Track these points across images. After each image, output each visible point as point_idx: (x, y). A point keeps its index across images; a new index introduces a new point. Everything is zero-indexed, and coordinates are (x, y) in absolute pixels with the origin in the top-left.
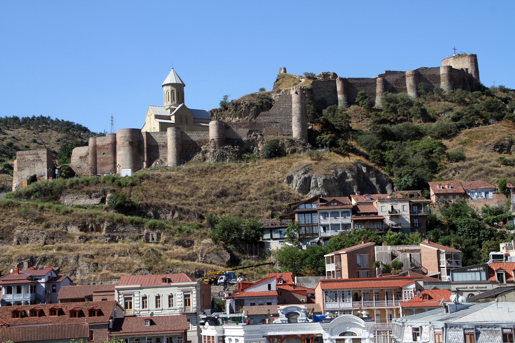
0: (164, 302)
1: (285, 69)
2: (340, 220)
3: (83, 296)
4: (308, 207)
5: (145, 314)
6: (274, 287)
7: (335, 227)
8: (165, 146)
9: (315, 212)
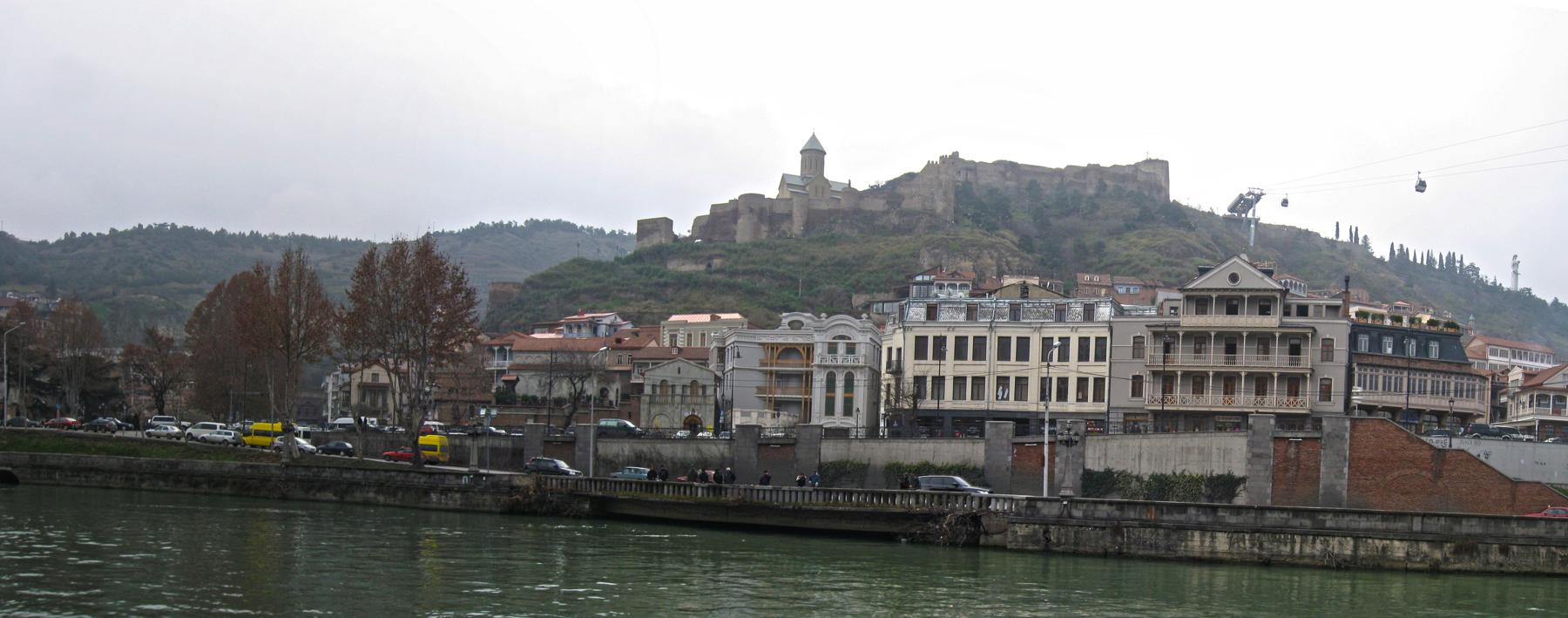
8: (789, 216)
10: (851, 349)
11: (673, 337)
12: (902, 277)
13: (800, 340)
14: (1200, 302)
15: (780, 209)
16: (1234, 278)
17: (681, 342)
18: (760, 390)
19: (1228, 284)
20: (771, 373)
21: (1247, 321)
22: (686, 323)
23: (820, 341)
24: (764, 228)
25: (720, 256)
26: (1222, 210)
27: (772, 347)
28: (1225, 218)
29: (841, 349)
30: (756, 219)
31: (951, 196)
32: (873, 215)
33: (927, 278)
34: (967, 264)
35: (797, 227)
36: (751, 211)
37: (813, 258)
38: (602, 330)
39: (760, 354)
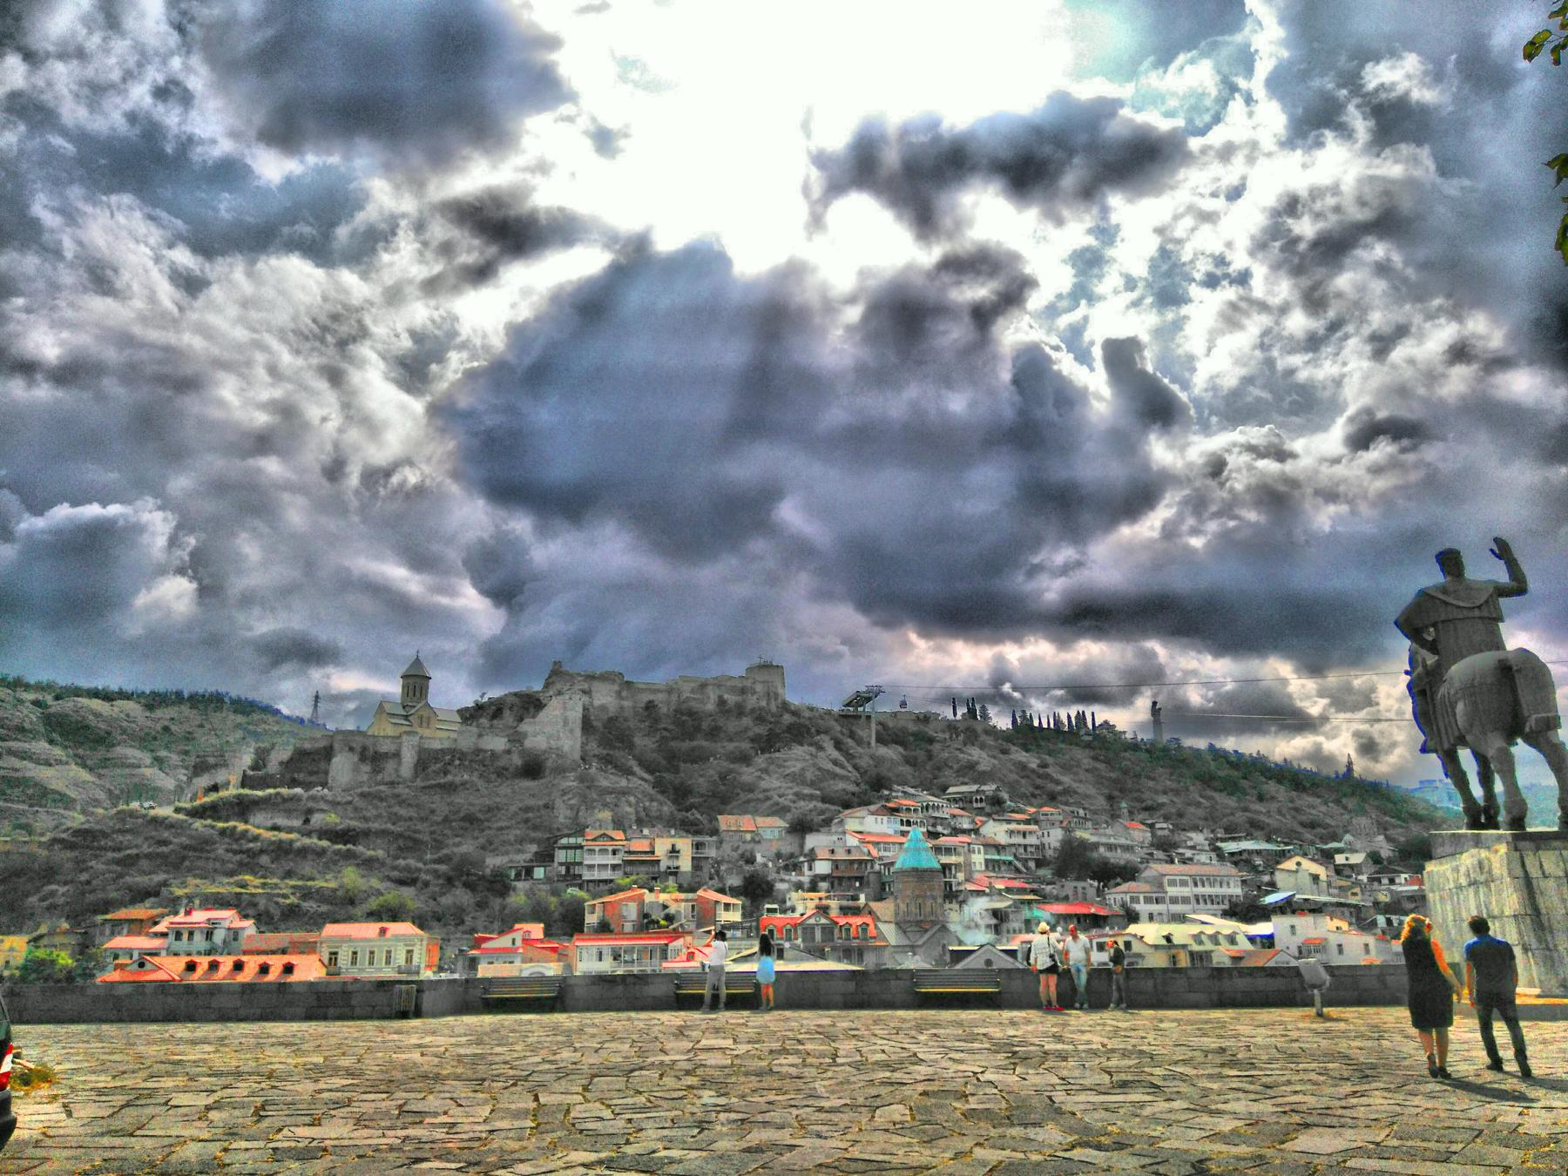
0: (380, 957)
3: (274, 948)
4: (572, 840)
5: (354, 973)
6: (519, 943)
8: (397, 755)
9: (581, 847)
11: (334, 955)
17: (344, 960)
22: (348, 939)
24: (366, 768)
26: (836, 708)
30: (356, 758)
31: (578, 733)
33: (572, 840)
34: (606, 815)
35: (406, 769)
37: (433, 812)
38: (219, 936)
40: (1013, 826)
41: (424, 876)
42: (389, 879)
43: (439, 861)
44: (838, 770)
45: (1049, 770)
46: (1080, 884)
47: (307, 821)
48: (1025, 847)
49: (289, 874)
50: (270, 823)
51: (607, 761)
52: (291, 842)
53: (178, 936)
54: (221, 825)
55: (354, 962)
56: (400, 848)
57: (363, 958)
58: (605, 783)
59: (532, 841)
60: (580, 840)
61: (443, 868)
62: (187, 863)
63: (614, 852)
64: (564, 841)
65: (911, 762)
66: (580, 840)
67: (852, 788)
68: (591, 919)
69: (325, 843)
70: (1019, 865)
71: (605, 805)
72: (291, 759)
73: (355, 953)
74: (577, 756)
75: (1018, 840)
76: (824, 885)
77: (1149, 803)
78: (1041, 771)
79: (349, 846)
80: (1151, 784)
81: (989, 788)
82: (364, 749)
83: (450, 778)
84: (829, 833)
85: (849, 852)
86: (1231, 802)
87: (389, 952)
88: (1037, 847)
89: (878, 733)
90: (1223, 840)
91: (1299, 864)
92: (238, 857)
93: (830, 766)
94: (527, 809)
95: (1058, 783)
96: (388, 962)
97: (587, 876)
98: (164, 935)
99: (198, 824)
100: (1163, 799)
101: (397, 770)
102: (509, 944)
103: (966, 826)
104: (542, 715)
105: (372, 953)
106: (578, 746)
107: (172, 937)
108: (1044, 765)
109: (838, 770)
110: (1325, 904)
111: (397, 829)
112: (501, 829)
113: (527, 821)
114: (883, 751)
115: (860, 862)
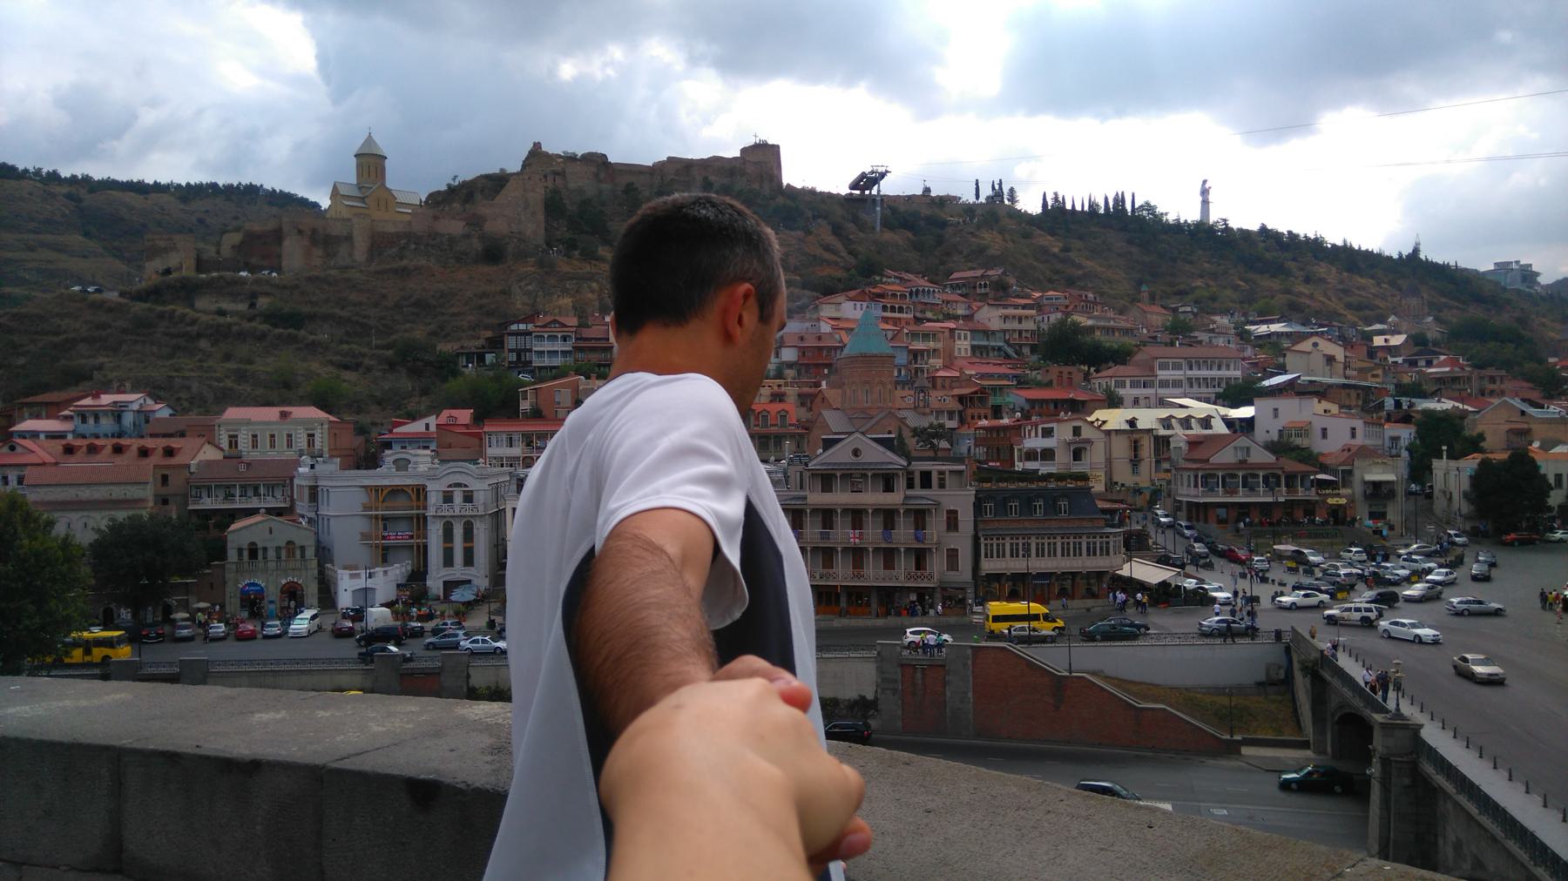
0: (281, 441)
1: (537, 146)
2: (559, 346)
4: (522, 327)
5: (255, 455)
6: (433, 428)
7: (553, 353)
8: (349, 238)
9: (530, 334)
10: (468, 498)
11: (233, 441)
12: (495, 321)
13: (409, 482)
14: (826, 480)
15: (337, 230)
16: (856, 452)
18: (365, 536)
19: (854, 459)
20: (376, 517)
21: (873, 497)
22: (248, 423)
23: (435, 490)
25: (267, 294)
26: (844, 190)
27: (377, 489)
28: (849, 199)
29: (458, 497)
31: (541, 217)
32: (452, 240)
33: (522, 327)
35: (360, 254)
36: (300, 232)
37: (384, 297)
38: (128, 419)
39: (362, 498)
40: (1011, 311)
41: (367, 361)
42: (331, 363)
43: (387, 347)
44: (827, 256)
45: (1072, 255)
46: (1066, 369)
47: (252, 305)
48: (1020, 332)
49: (227, 357)
50: (214, 307)
51: (571, 245)
52: (230, 325)
53: (84, 420)
54: (160, 308)
55: (255, 446)
56: (348, 334)
57: (264, 441)
58: (566, 269)
59: (487, 328)
60: (530, 327)
61: (390, 352)
62: (124, 347)
63: (564, 339)
64: (514, 327)
65: (917, 247)
66: (530, 327)
67: (840, 274)
68: (525, 406)
69: (265, 327)
70: (1010, 351)
71: (565, 292)
72: (242, 242)
73: (255, 436)
74: (541, 240)
75: (1015, 325)
76: (790, 373)
77: (1182, 287)
78: (1062, 255)
79: (291, 331)
80: (1188, 267)
81: (995, 273)
82: (314, 231)
83: (405, 262)
84: (803, 320)
85: (820, 338)
86: (1275, 284)
87: (289, 436)
88: (1033, 332)
89: (884, 218)
90: (1253, 323)
91: (1315, 345)
92: (174, 341)
93: (819, 251)
94: (484, 295)
95: (1080, 267)
96: (290, 445)
97: (537, 362)
98: (71, 417)
99: (139, 307)
100: (1199, 283)
101: (351, 255)
102: (423, 429)
103: (960, 312)
104: (500, 199)
105: (272, 436)
106: (543, 231)
107: (77, 421)
108: (1066, 249)
109: (827, 256)
110: (1330, 386)
111: (344, 313)
112: (454, 315)
113: (481, 307)
114: (888, 236)
115: (830, 349)
